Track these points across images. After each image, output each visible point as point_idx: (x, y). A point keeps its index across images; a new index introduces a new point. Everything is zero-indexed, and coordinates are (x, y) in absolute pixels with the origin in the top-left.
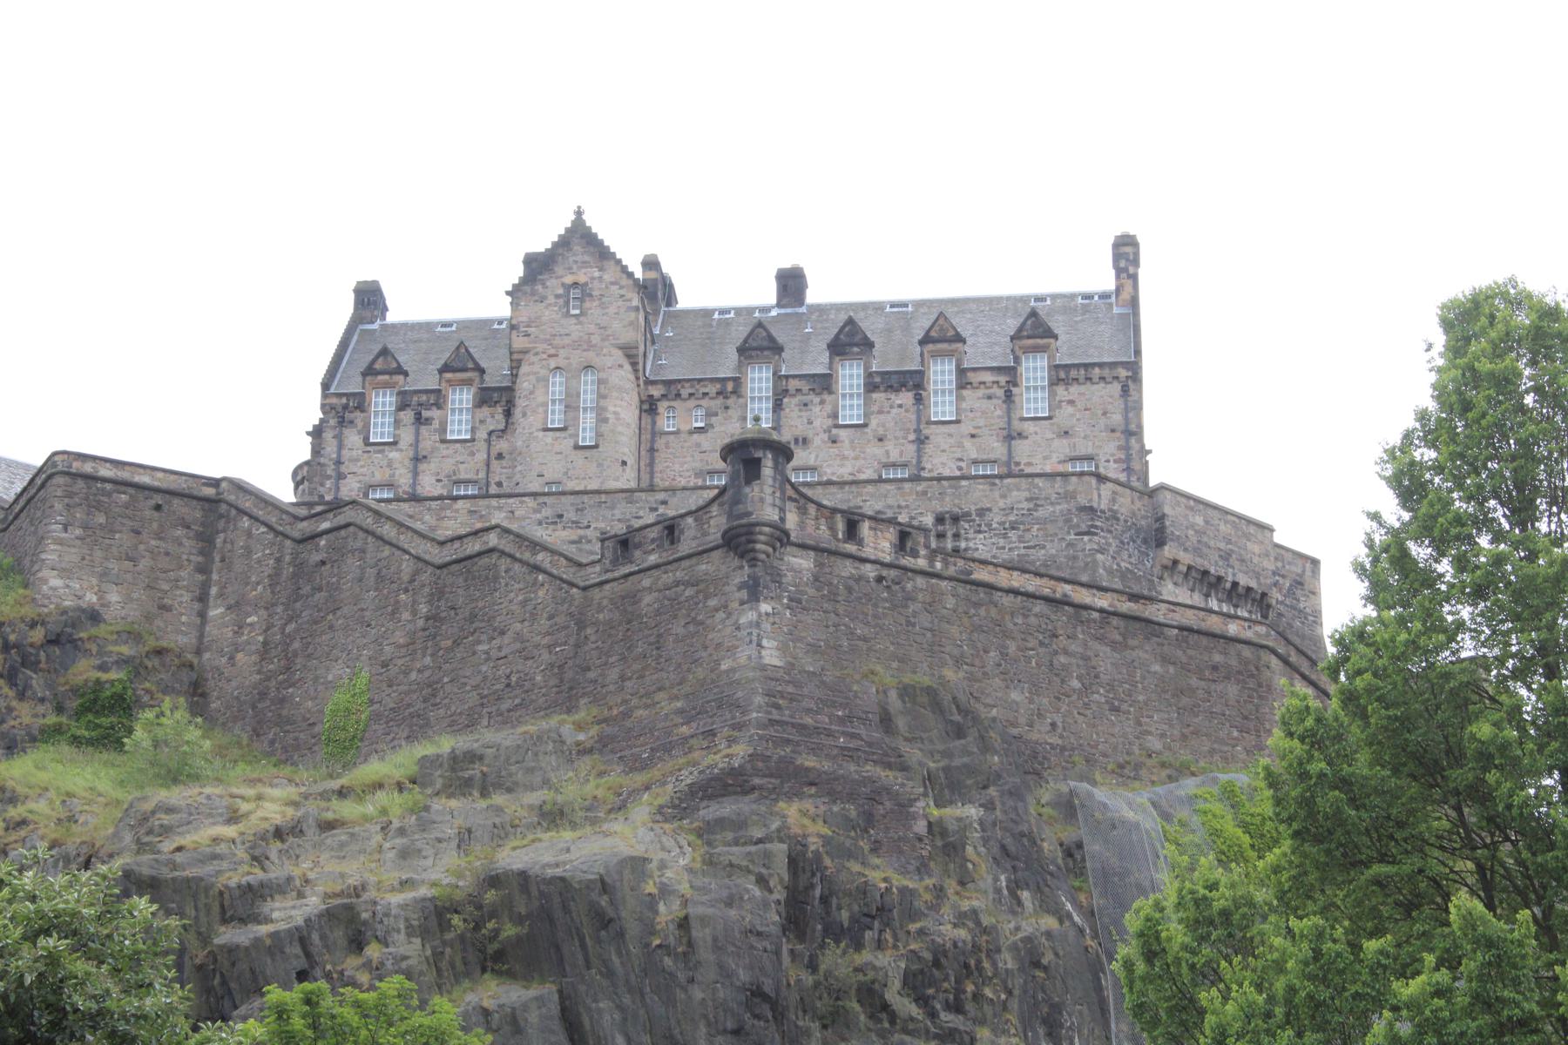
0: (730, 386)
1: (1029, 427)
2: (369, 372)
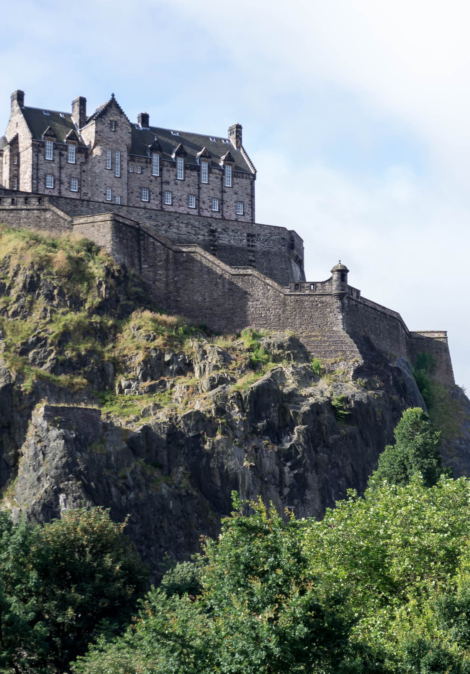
0: (149, 161)
1: (227, 190)
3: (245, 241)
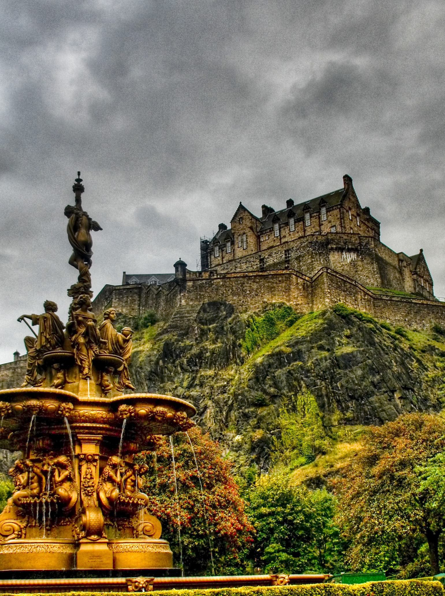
1: (323, 222)
3: (284, 256)
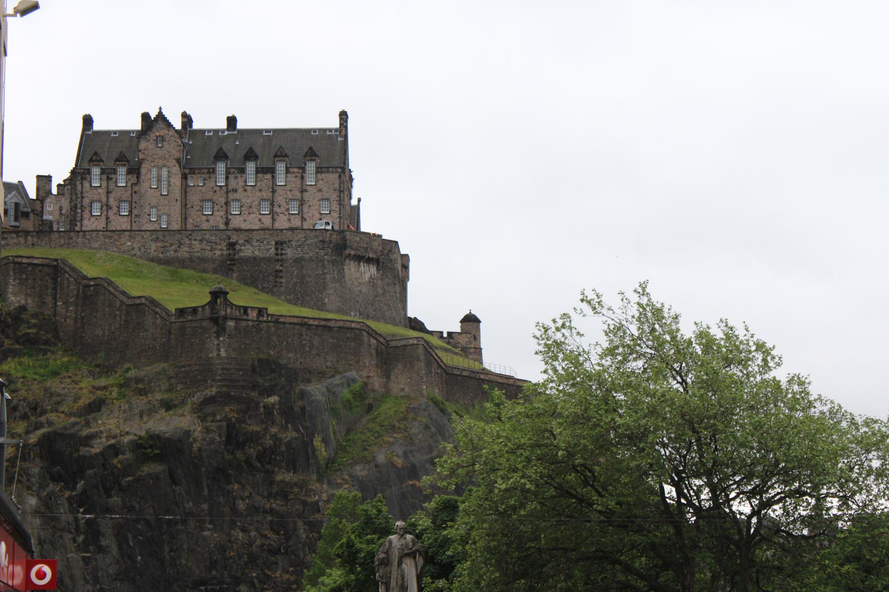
1: (309, 188)
2: (91, 161)
3: (273, 249)
